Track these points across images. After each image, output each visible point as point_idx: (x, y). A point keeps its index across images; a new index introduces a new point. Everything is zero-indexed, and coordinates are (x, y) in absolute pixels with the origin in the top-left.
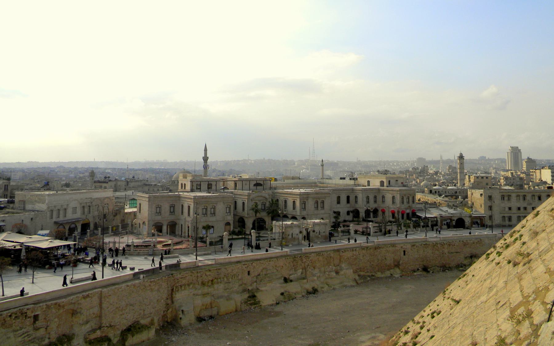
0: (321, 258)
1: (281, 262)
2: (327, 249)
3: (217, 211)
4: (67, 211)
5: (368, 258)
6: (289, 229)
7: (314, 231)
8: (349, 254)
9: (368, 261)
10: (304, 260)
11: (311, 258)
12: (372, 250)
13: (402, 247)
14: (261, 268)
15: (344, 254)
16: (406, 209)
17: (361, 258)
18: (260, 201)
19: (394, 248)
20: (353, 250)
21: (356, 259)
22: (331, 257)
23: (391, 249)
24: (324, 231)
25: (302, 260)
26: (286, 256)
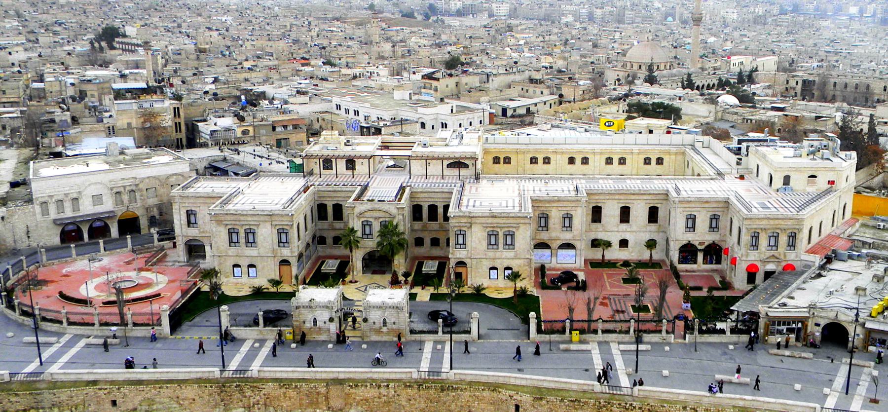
0: (292, 393)
1: (190, 392)
2: (318, 376)
3: (259, 238)
5: (423, 405)
6: (303, 311)
7: (365, 320)
8: (361, 393)
10: (248, 393)
11: (263, 391)
12: (432, 392)
13: (511, 397)
14: (140, 398)
15: (352, 391)
16: (765, 262)
17: (404, 403)
18: (376, 218)
19: (495, 394)
20: (379, 387)
21: (388, 403)
22: (318, 393)
23: (486, 393)
24: (393, 320)
25: (242, 392)
26: (199, 381)
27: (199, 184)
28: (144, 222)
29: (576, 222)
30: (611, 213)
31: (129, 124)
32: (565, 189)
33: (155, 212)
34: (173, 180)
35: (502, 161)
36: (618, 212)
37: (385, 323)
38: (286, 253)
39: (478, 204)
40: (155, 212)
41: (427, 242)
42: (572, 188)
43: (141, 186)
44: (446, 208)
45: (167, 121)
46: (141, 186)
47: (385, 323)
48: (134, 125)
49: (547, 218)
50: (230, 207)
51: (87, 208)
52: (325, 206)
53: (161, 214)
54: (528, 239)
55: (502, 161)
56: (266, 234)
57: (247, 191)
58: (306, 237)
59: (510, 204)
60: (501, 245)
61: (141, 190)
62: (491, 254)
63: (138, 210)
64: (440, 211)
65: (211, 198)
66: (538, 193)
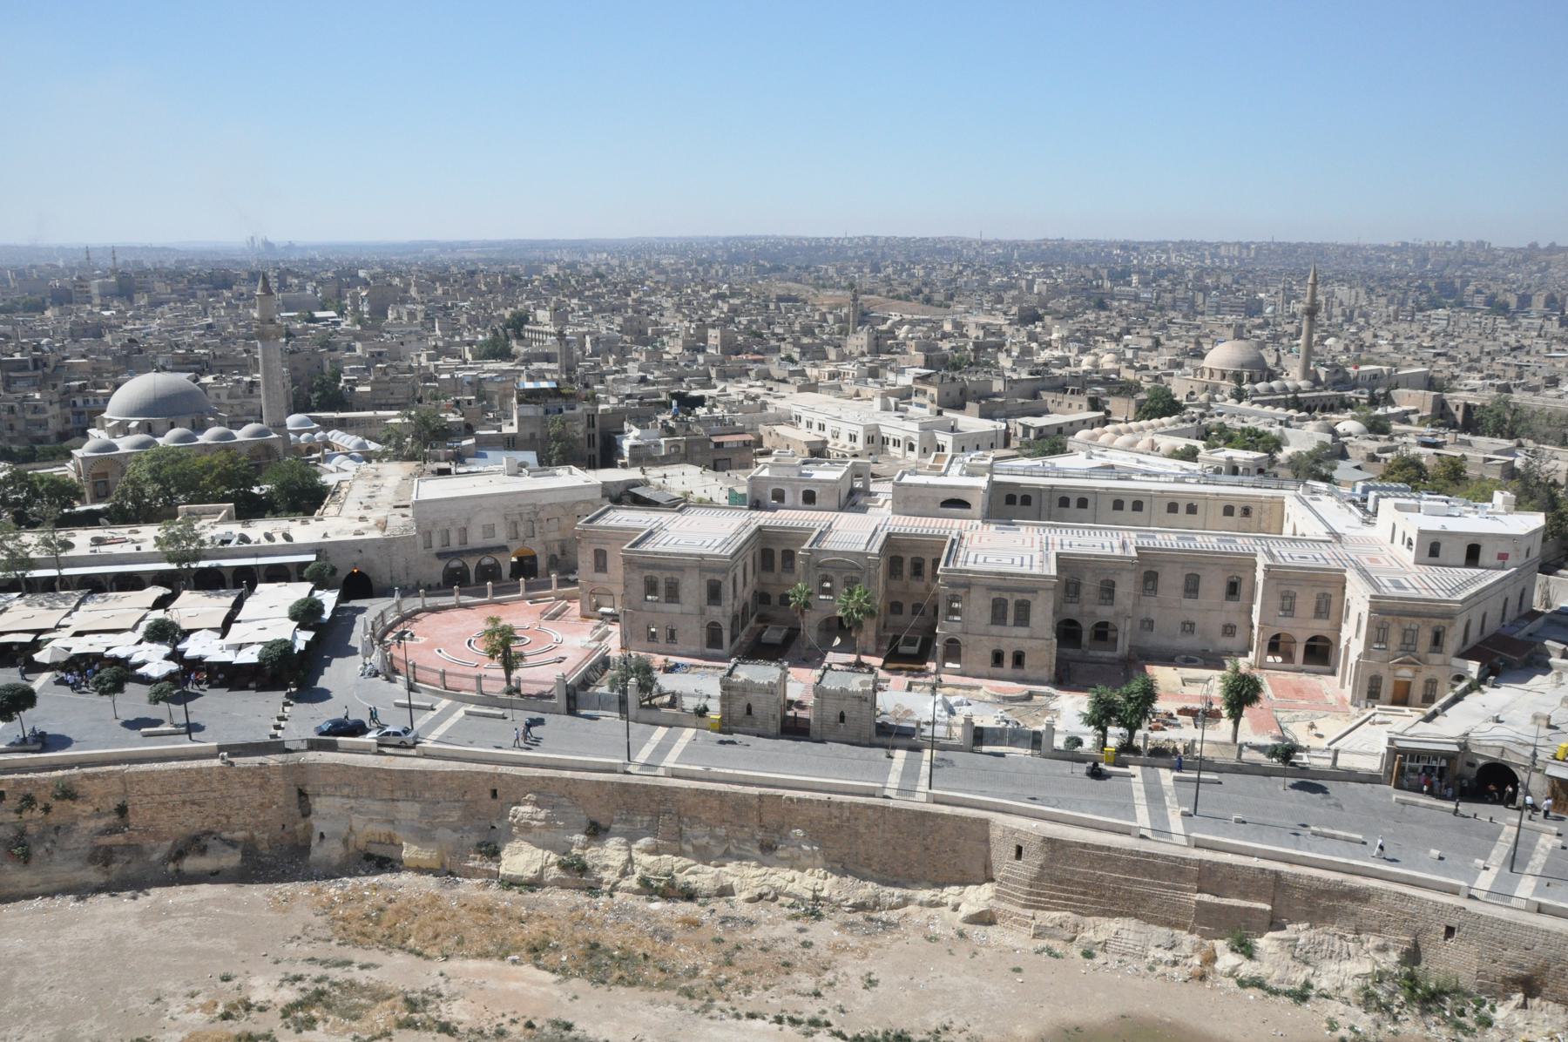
4: (469, 531)
9: (887, 842)
17: (862, 830)
27: (611, 514)
28: (542, 563)
29: (1119, 591)
30: (1172, 581)
31: (532, 435)
32: (1107, 544)
33: (557, 551)
34: (580, 508)
35: (1018, 501)
36: (1181, 582)
37: (842, 718)
38: (715, 613)
39: (980, 559)
40: (557, 551)
41: (908, 608)
42: (1116, 543)
43: (541, 515)
44: (936, 562)
45: (580, 430)
46: (541, 515)
47: (842, 718)
48: (538, 436)
49: (1078, 585)
50: (648, 547)
51: (476, 539)
52: (772, 551)
53: (563, 553)
54: (1050, 614)
55: (1018, 501)
56: (693, 589)
57: (672, 527)
58: (746, 594)
59: (1027, 561)
60: (1010, 619)
61: (540, 521)
62: (995, 629)
63: (535, 547)
64: (928, 566)
65: (623, 533)
66: (1067, 549)
